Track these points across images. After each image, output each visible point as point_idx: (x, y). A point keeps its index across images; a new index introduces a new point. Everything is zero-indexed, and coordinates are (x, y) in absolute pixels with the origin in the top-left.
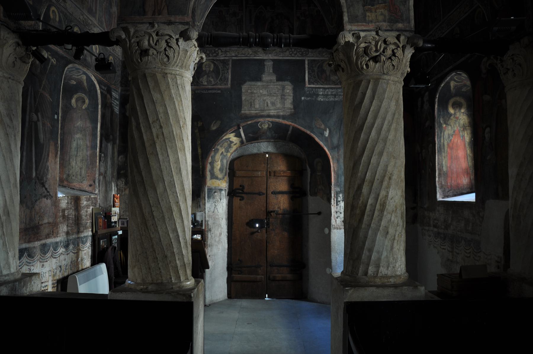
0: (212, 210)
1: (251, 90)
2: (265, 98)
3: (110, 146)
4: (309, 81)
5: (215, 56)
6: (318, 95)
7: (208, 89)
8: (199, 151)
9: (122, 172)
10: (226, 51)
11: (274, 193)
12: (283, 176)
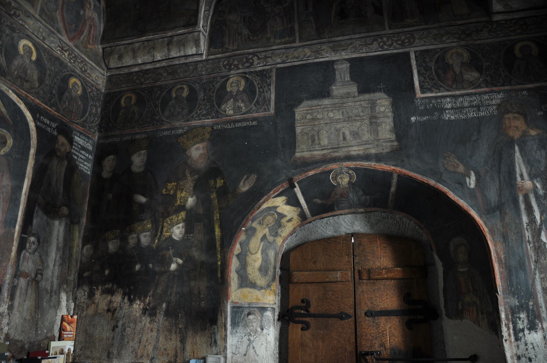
0: (243, 350)
1: (311, 114)
2: (339, 126)
3: (58, 228)
4: (421, 87)
5: (248, 67)
6: (442, 110)
7: (235, 121)
8: (218, 232)
9: (86, 274)
10: (266, 57)
11: (370, 314)
12: (387, 279)
